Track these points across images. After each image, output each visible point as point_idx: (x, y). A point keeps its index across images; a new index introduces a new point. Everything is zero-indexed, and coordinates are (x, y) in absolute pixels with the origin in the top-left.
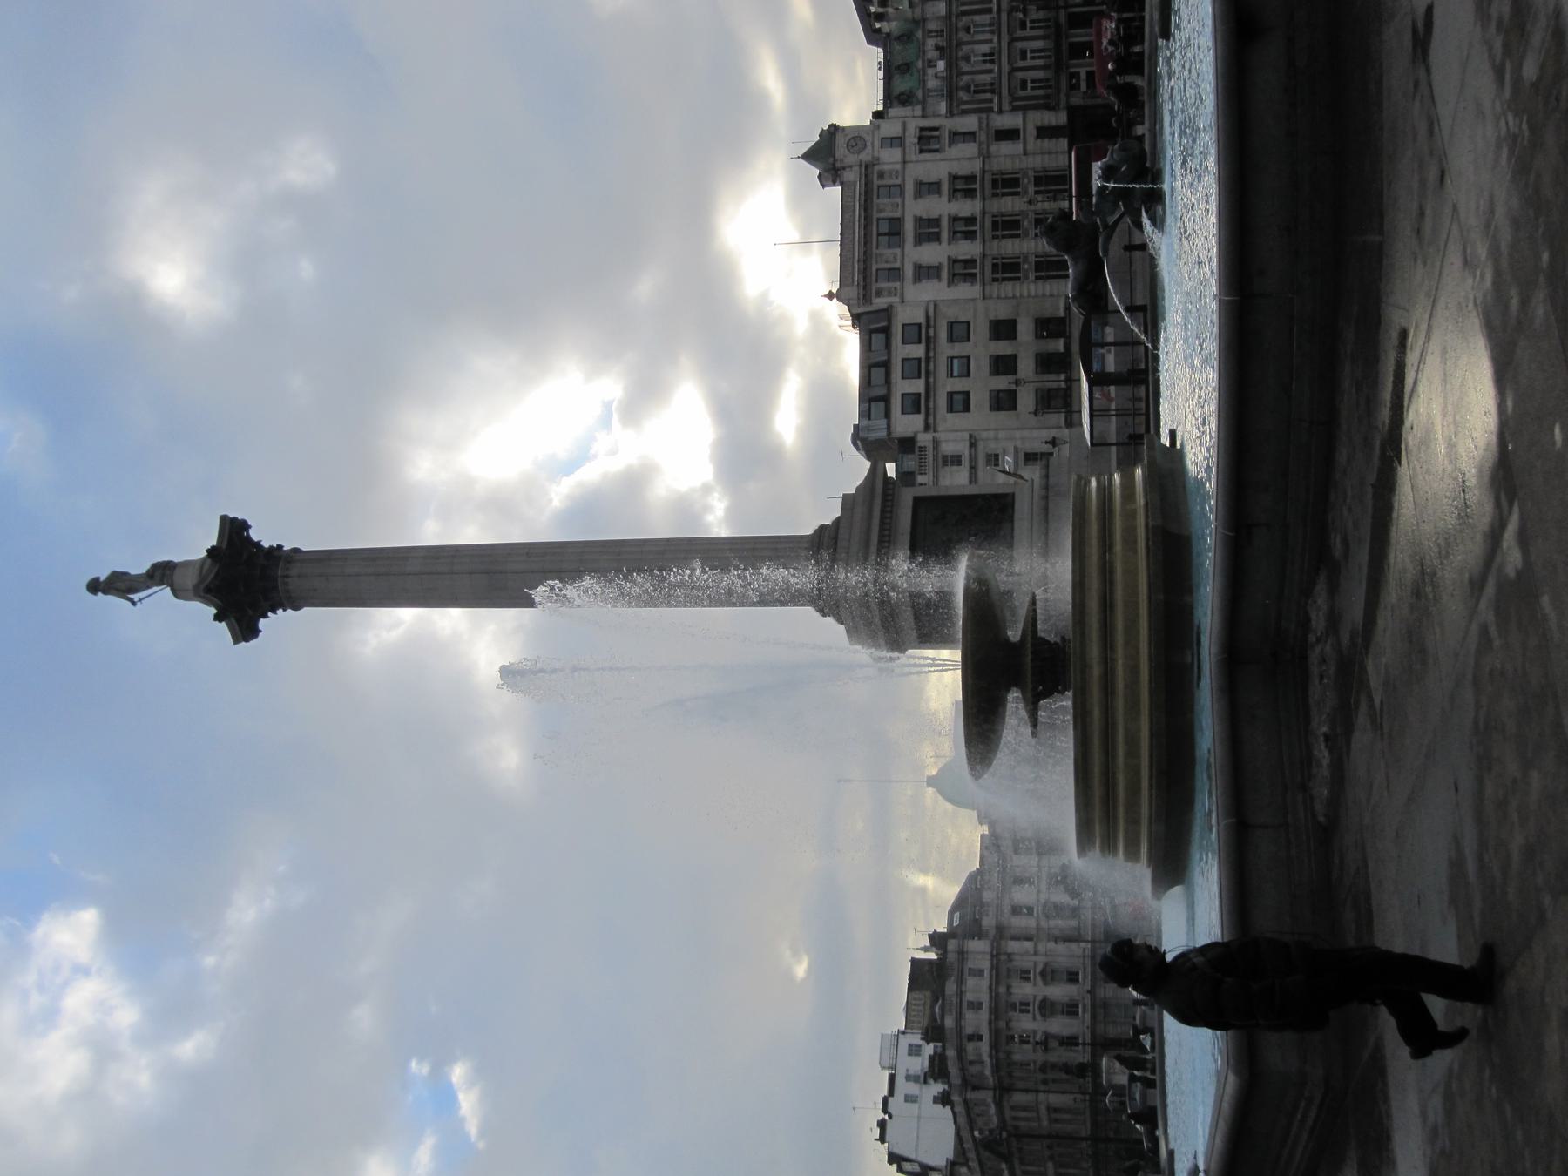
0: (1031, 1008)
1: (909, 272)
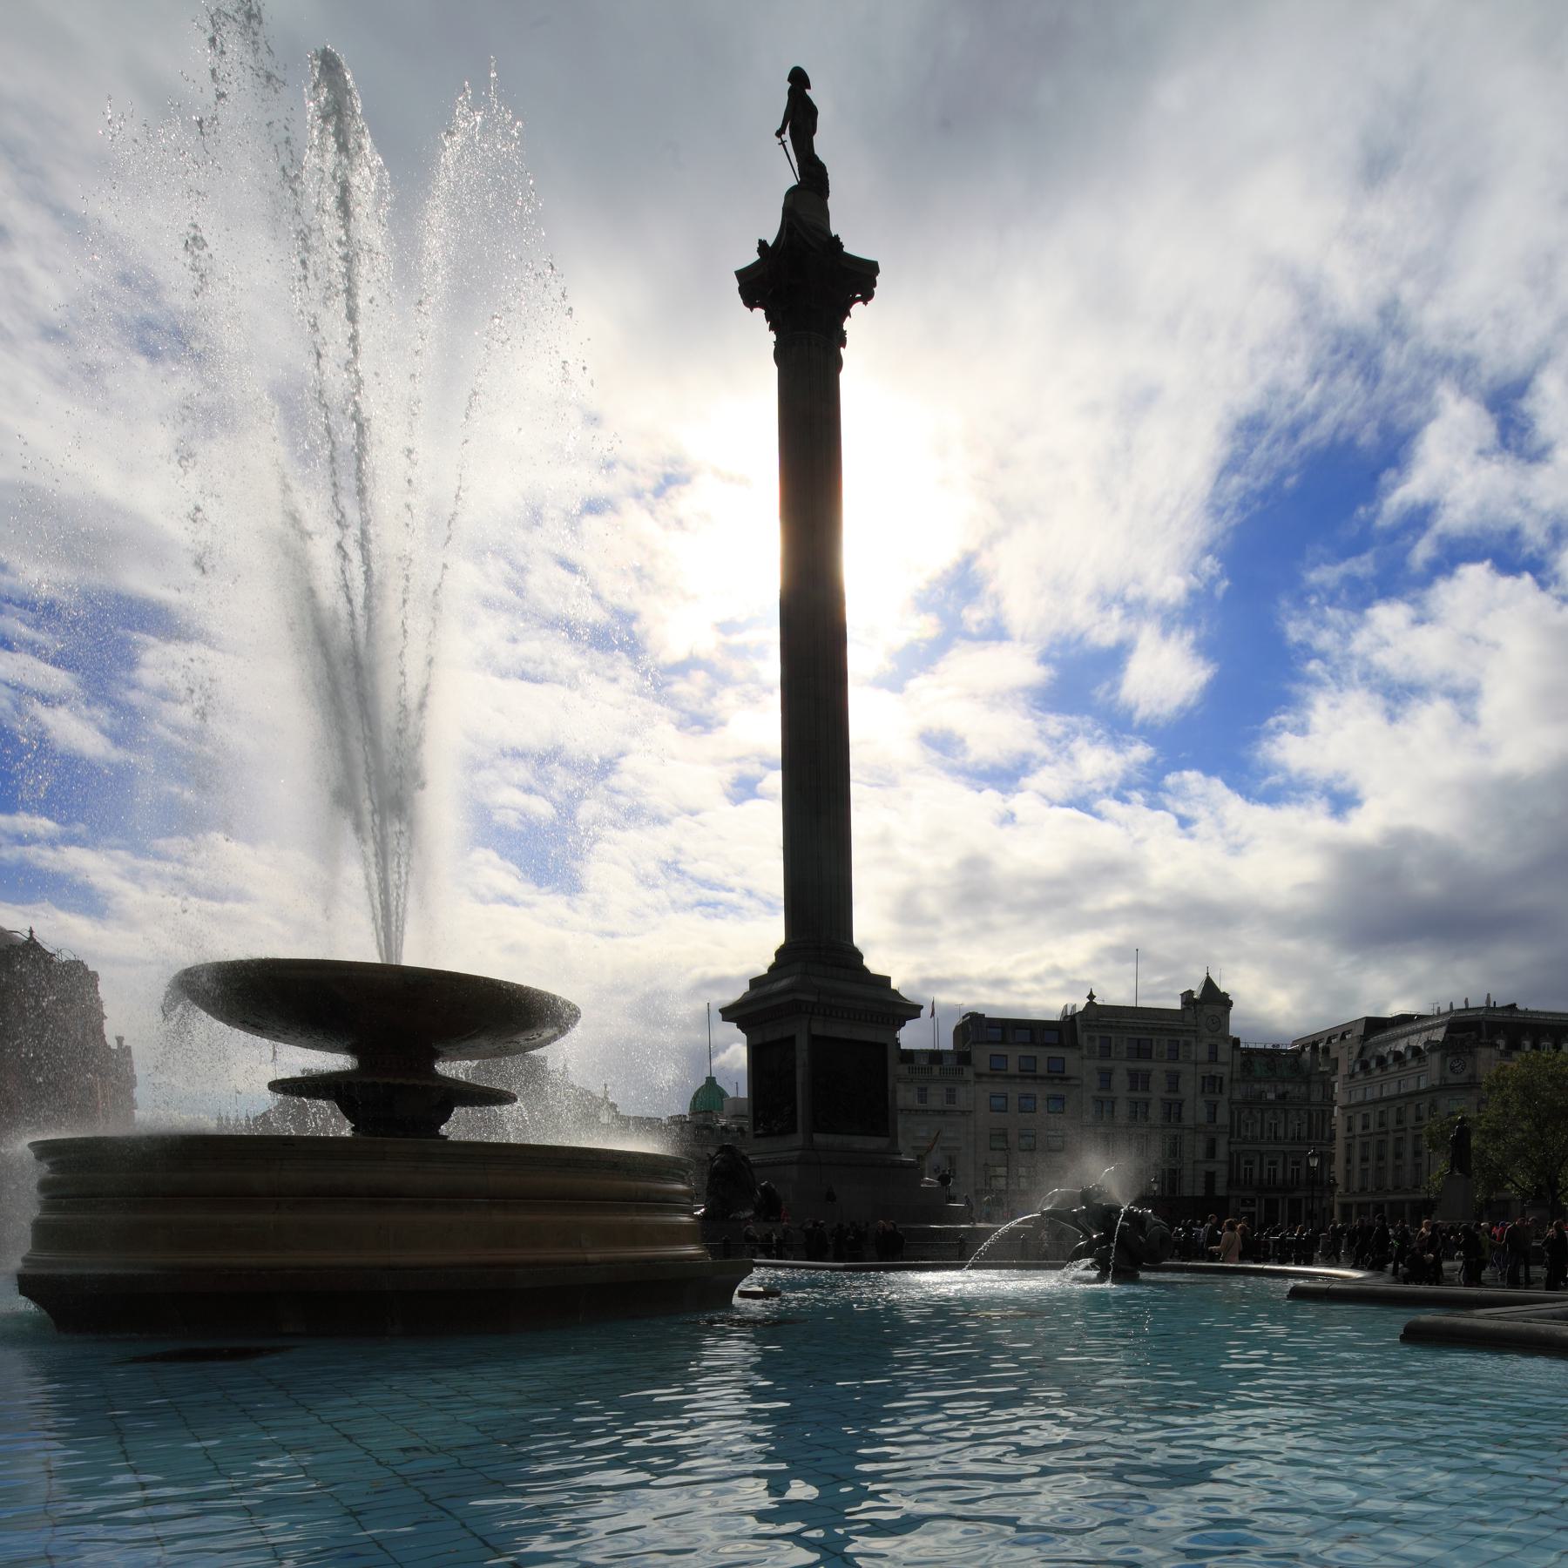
1: (1107, 1064)
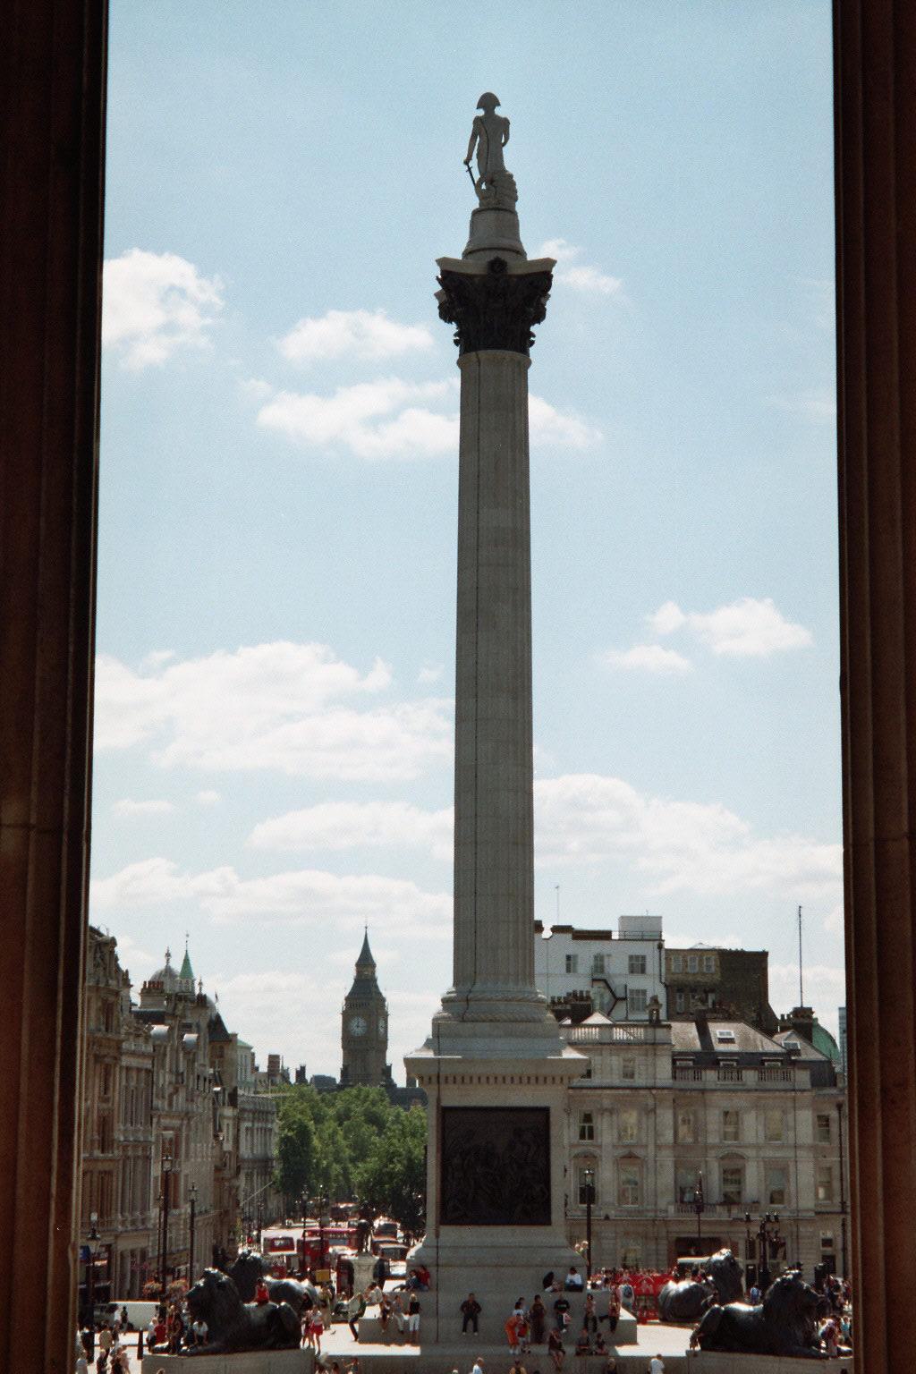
0: (587, 1141)
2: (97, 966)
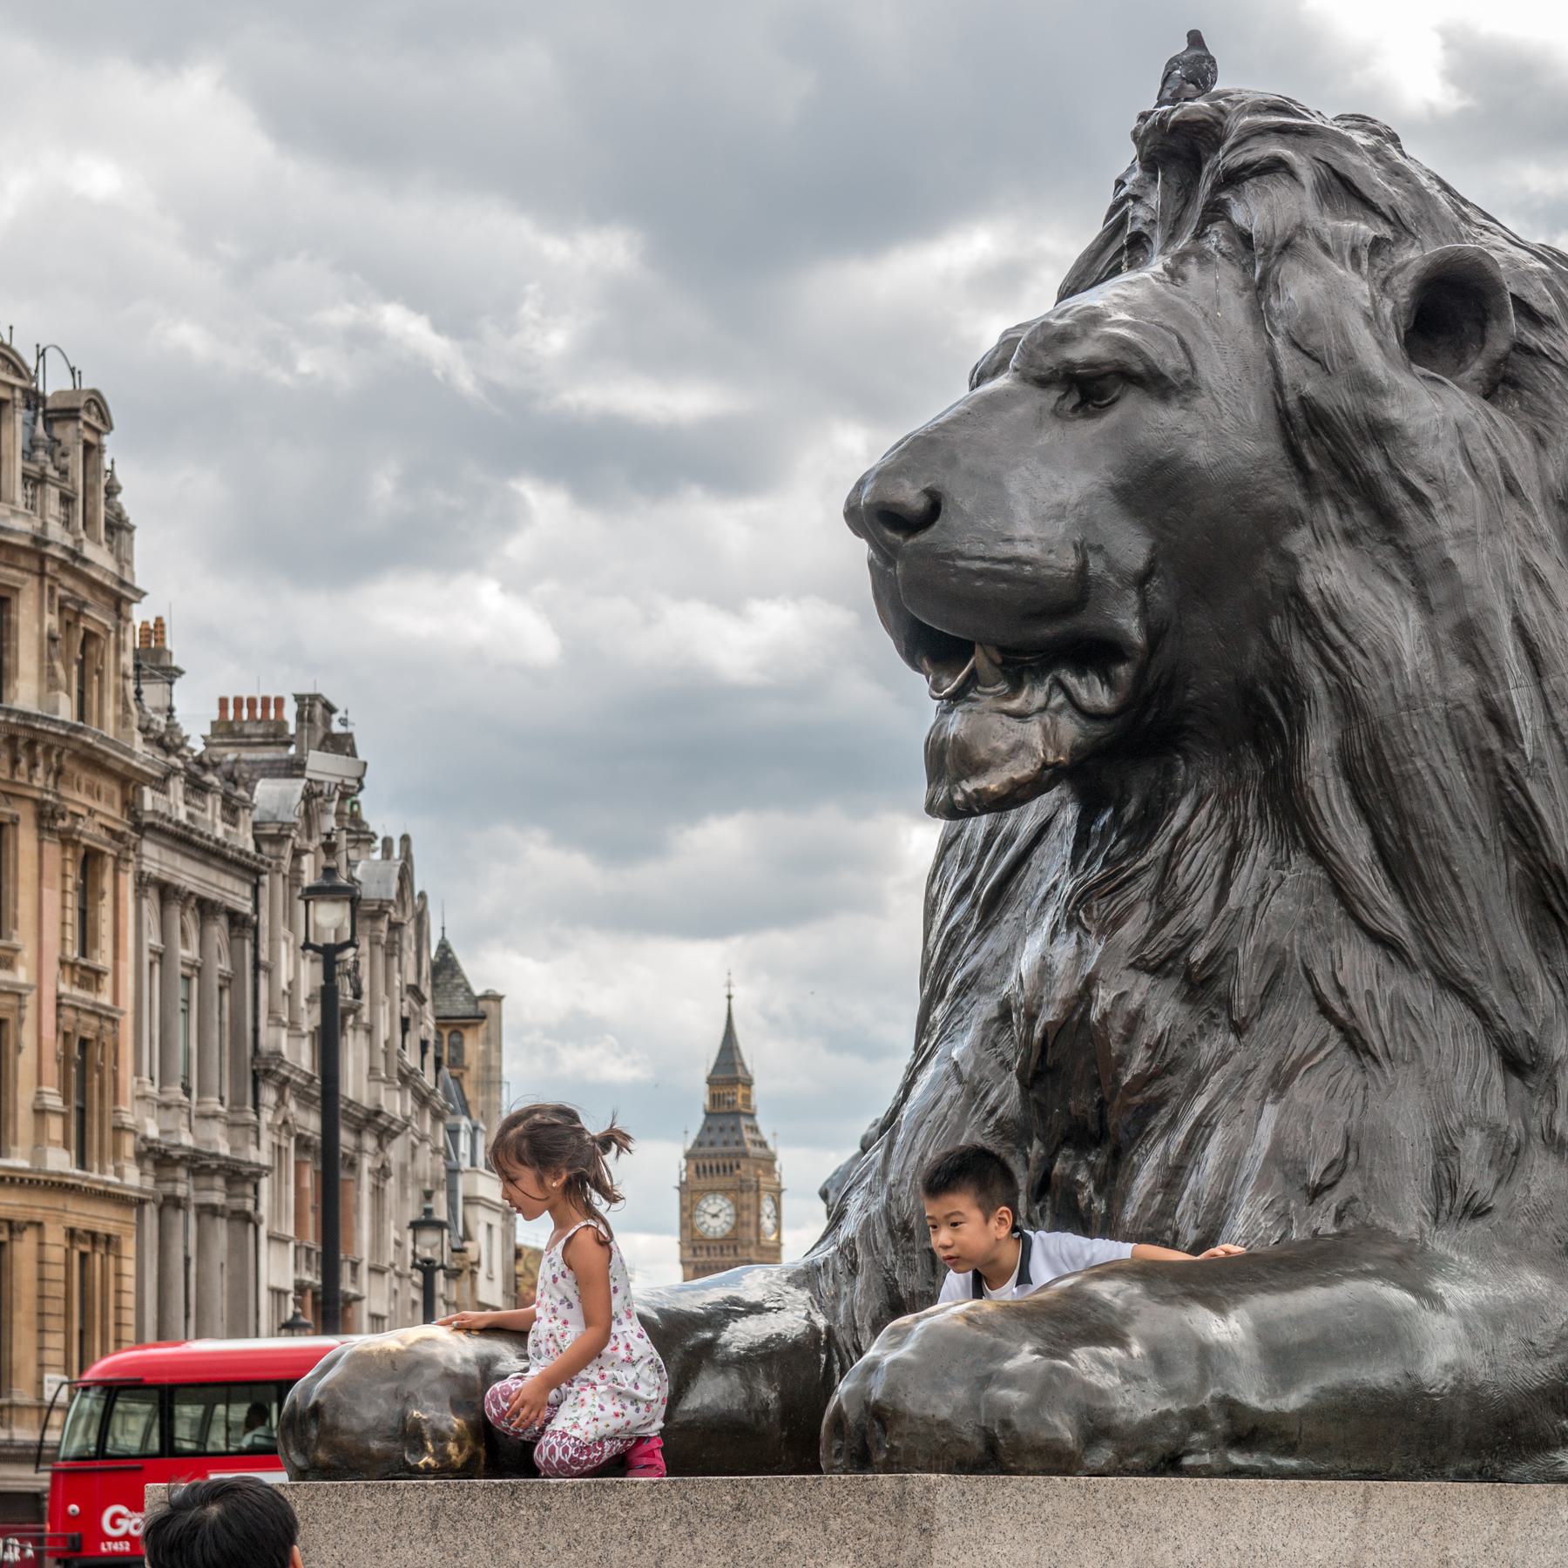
2: (35, 481)
